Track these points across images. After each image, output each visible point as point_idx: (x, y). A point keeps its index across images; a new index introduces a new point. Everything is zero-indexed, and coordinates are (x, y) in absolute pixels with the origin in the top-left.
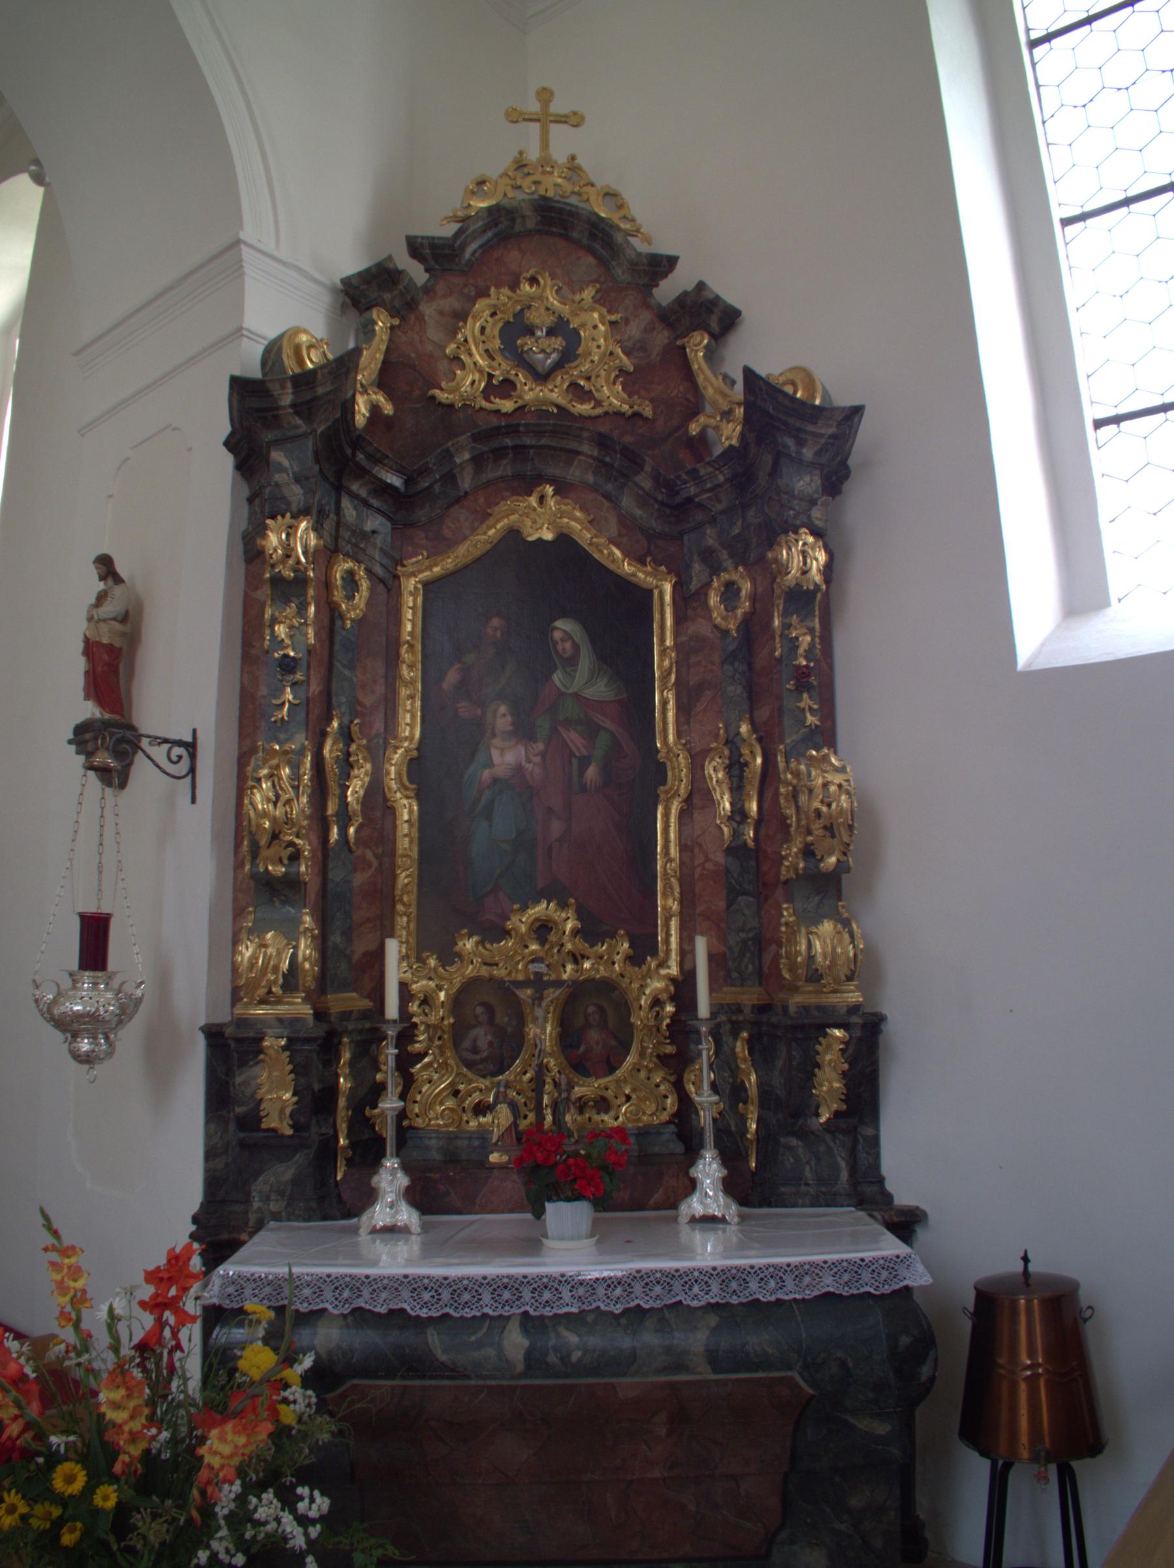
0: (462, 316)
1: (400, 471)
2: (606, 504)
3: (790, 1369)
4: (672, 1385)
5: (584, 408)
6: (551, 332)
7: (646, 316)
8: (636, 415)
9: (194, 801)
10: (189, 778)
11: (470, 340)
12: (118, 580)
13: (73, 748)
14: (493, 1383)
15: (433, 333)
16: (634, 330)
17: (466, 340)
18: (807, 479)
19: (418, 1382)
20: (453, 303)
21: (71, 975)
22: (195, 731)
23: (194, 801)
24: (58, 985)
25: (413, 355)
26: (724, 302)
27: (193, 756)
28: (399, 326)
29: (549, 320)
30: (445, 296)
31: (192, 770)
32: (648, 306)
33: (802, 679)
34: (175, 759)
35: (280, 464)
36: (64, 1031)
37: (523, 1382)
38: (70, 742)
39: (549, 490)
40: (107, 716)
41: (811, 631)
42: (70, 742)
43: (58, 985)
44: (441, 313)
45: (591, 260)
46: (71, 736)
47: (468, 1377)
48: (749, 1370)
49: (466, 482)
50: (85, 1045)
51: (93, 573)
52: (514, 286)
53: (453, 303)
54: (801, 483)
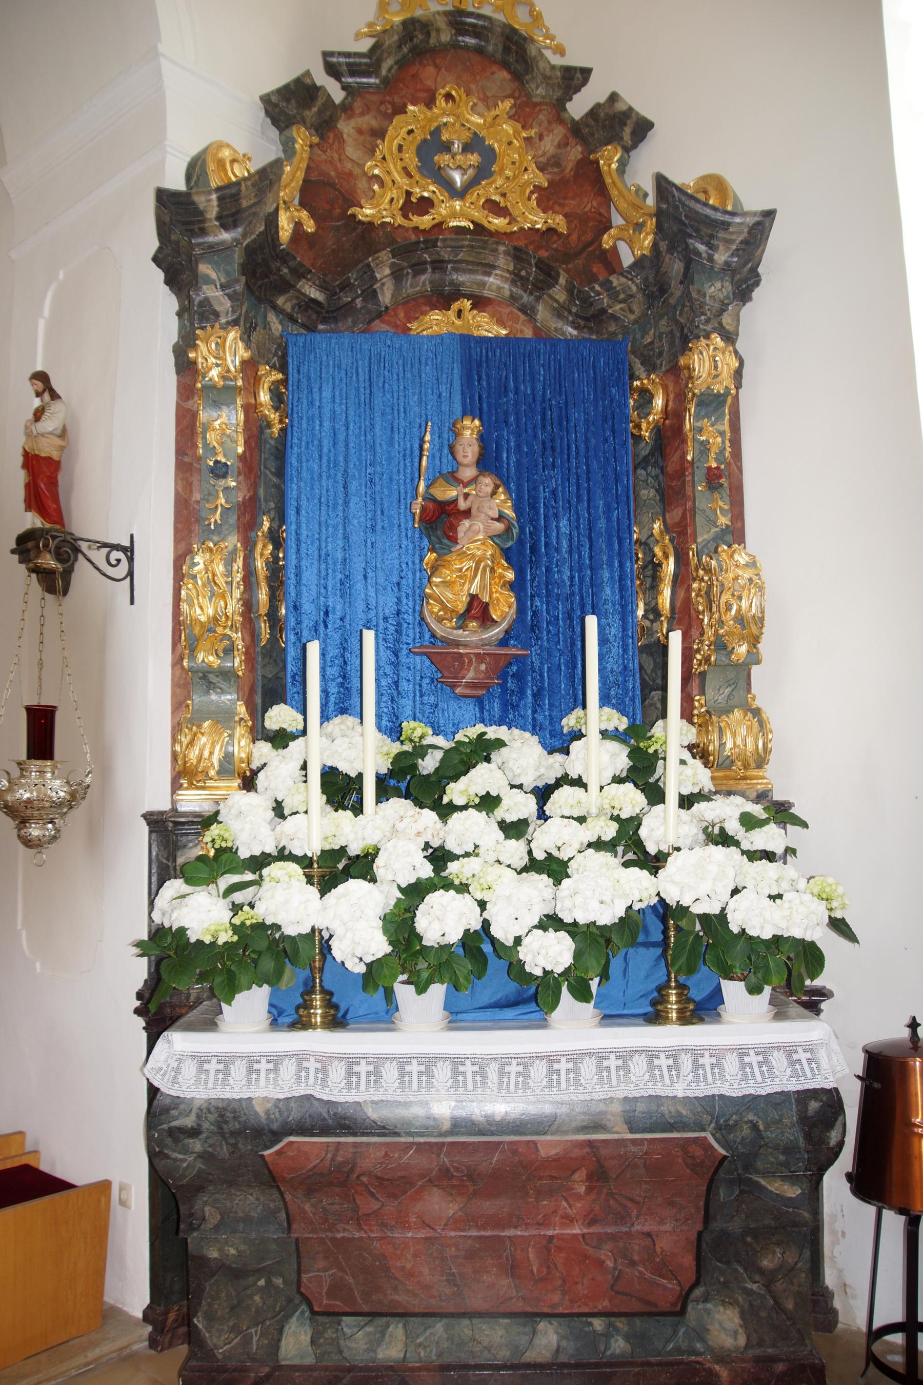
0: (381, 134)
1: (323, 287)
2: (522, 317)
3: (704, 1130)
4: (590, 1143)
5: (498, 222)
6: (467, 148)
7: (559, 132)
8: (551, 231)
9: (132, 602)
10: (129, 578)
11: (387, 157)
12: (54, 396)
13: (16, 557)
14: (422, 1140)
15: (351, 151)
16: (548, 145)
17: (384, 158)
18: (718, 285)
19: (351, 1139)
20: (370, 121)
21: (19, 764)
22: (132, 536)
23: (132, 602)
24: (8, 773)
25: (333, 173)
26: (637, 113)
27: (131, 560)
28: (318, 145)
29: (466, 136)
30: (362, 114)
31: (131, 574)
32: (560, 120)
33: (713, 479)
34: (114, 562)
35: (207, 276)
36: (14, 818)
37: (450, 1139)
38: (13, 552)
39: (468, 304)
40: (48, 526)
41: (722, 434)
42: (13, 552)
43: (8, 773)
44: (360, 131)
45: (505, 75)
46: (14, 546)
47: (397, 1134)
48: (663, 1131)
49: (386, 296)
50: (35, 831)
51: (28, 390)
52: (430, 103)
53: (370, 121)
54: (713, 288)
